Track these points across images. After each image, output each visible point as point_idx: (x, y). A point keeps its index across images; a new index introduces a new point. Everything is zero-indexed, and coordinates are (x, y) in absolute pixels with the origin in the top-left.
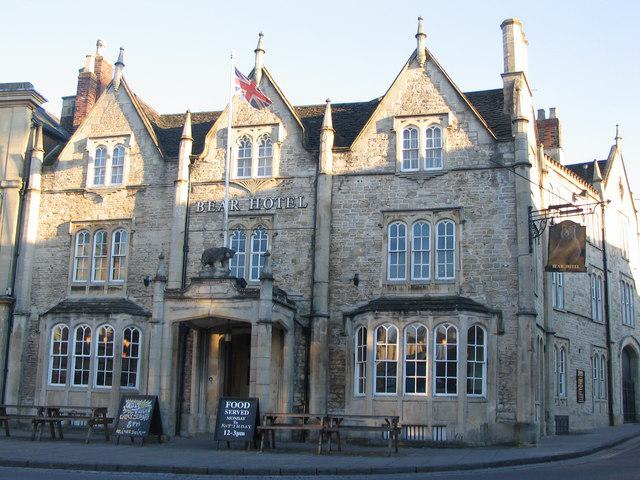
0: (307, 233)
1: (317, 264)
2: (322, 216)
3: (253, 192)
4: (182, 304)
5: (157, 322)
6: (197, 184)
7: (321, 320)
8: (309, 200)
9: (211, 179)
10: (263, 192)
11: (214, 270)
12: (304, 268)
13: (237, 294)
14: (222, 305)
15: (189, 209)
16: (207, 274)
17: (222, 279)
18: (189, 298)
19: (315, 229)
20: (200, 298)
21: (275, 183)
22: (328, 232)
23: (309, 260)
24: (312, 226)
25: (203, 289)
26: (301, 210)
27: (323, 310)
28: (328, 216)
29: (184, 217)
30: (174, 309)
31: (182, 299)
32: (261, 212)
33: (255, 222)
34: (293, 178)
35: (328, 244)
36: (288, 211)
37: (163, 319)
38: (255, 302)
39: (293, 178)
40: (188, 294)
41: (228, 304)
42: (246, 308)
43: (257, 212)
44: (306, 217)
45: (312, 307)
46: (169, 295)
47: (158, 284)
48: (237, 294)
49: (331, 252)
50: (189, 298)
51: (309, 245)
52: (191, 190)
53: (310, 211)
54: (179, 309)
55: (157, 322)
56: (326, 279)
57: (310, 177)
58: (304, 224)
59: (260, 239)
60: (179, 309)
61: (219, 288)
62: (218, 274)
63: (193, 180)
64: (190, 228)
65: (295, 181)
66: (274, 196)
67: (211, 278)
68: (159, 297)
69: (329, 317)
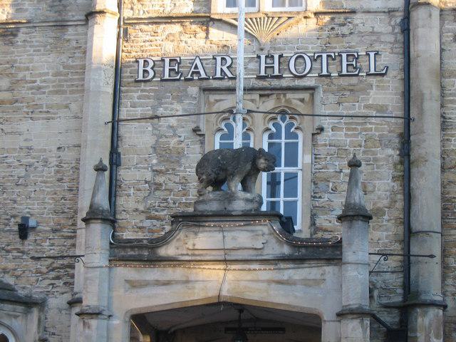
0: (389, 128)
1: (416, 192)
2: (426, 92)
3: (265, 39)
4: (152, 274)
5: (96, 314)
6: (138, 21)
7: (434, 313)
8: (390, 59)
9: (169, 10)
10: (287, 41)
11: (231, 197)
12: (386, 202)
13: (286, 250)
14: (249, 276)
15: (118, 68)
16: (214, 207)
17: (252, 216)
18: (172, 261)
19: (408, 120)
20: (196, 260)
21: (312, 23)
22: (438, 128)
23: (397, 186)
24: (400, 113)
25: (204, 240)
26: (373, 80)
27: (433, 290)
28: (437, 93)
29: (111, 90)
30: (134, 285)
31: (155, 261)
32: (284, 83)
33: (270, 104)
34: (353, 12)
35: (438, 151)
36: (344, 82)
37: (109, 307)
38: (330, 270)
39: (353, 12)
40: (168, 251)
41: (266, 273)
42: (307, 283)
43: (275, 83)
44: (386, 95)
45: (407, 285)
46: (123, 252)
47: (97, 227)
48: (286, 250)
49: (443, 169)
50: (172, 261)
51: (393, 153)
52: (123, 34)
53: (393, 82)
54: (145, 284)
55: (96, 314)
56: (438, 228)
57: (390, 12)
58: (381, 109)
59: (283, 141)
60: (145, 284)
61: (242, 238)
62: (239, 206)
63: (127, 13)
64: (123, 114)
65: (358, 19)
66: (312, 49)
67: (224, 216)
68: (99, 257)
69: (445, 307)
